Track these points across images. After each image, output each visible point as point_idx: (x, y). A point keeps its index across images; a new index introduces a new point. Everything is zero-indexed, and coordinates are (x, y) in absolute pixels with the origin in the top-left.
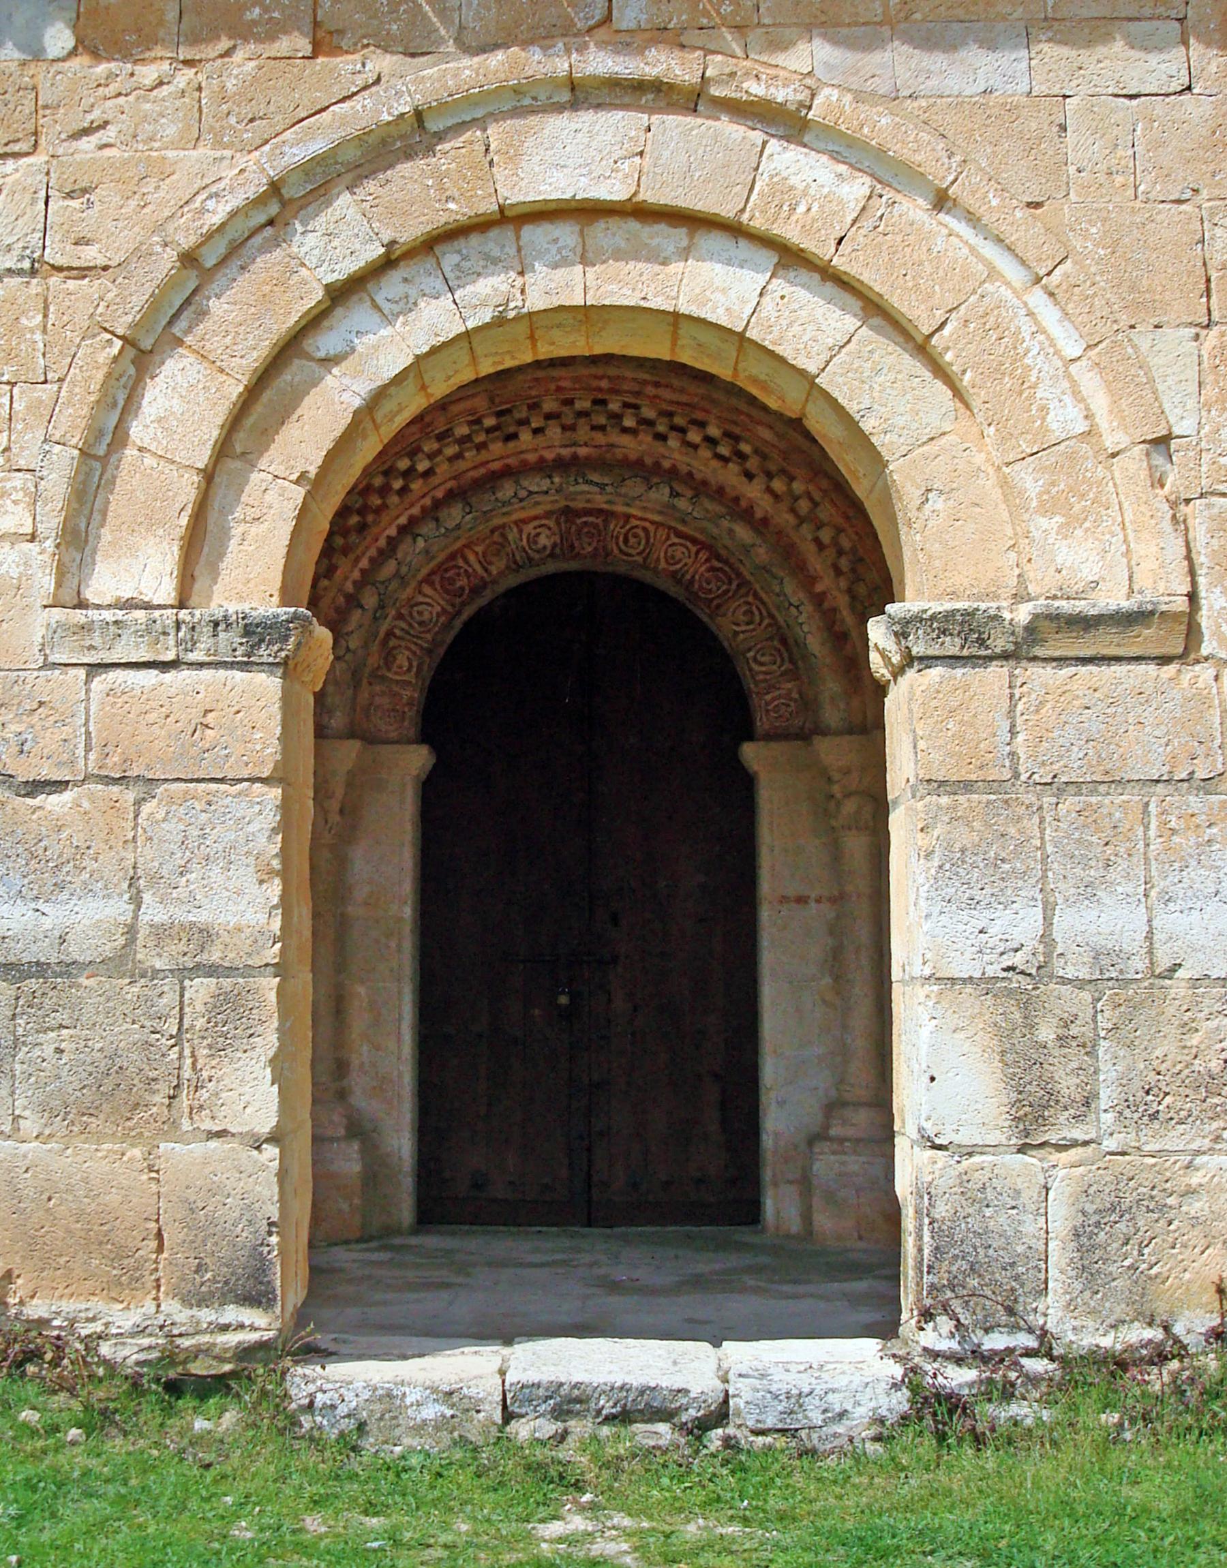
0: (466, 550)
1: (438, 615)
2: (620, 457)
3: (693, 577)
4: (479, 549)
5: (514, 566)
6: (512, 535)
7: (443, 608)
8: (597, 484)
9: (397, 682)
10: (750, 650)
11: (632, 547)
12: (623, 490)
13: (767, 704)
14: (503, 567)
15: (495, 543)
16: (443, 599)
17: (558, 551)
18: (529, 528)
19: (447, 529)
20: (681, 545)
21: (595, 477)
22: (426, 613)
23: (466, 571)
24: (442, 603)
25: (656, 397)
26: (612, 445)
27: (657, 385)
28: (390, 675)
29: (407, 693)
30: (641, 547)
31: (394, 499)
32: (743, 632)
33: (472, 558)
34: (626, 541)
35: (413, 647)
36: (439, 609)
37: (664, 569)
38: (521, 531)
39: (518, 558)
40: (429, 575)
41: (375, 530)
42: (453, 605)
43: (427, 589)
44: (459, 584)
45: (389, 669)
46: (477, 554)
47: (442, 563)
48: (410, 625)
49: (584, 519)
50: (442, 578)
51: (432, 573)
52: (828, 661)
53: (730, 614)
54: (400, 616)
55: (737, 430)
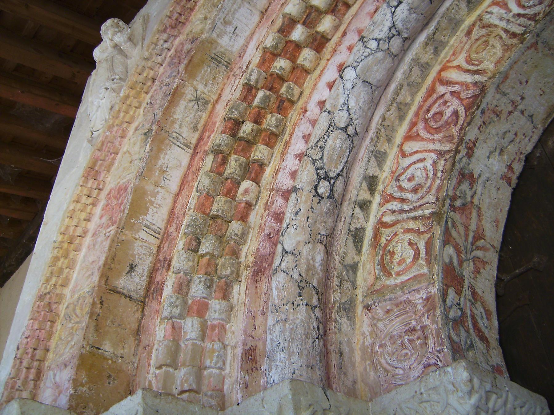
0: (443, 74)
4: (461, 60)
5: (515, 41)
9: (402, 286)
14: (499, 53)
16: (433, 141)
19: (378, 41)
22: (418, 173)
23: (452, 93)
24: (431, 146)
28: (391, 282)
29: (418, 298)
33: (453, 75)
35: (412, 225)
36: (433, 156)
40: (410, 129)
41: (300, 104)
42: (450, 139)
43: (410, 147)
44: (448, 112)
45: (390, 274)
46: (458, 67)
47: (420, 107)
48: (403, 200)
50: (426, 121)
51: (413, 124)
54: (388, 198)
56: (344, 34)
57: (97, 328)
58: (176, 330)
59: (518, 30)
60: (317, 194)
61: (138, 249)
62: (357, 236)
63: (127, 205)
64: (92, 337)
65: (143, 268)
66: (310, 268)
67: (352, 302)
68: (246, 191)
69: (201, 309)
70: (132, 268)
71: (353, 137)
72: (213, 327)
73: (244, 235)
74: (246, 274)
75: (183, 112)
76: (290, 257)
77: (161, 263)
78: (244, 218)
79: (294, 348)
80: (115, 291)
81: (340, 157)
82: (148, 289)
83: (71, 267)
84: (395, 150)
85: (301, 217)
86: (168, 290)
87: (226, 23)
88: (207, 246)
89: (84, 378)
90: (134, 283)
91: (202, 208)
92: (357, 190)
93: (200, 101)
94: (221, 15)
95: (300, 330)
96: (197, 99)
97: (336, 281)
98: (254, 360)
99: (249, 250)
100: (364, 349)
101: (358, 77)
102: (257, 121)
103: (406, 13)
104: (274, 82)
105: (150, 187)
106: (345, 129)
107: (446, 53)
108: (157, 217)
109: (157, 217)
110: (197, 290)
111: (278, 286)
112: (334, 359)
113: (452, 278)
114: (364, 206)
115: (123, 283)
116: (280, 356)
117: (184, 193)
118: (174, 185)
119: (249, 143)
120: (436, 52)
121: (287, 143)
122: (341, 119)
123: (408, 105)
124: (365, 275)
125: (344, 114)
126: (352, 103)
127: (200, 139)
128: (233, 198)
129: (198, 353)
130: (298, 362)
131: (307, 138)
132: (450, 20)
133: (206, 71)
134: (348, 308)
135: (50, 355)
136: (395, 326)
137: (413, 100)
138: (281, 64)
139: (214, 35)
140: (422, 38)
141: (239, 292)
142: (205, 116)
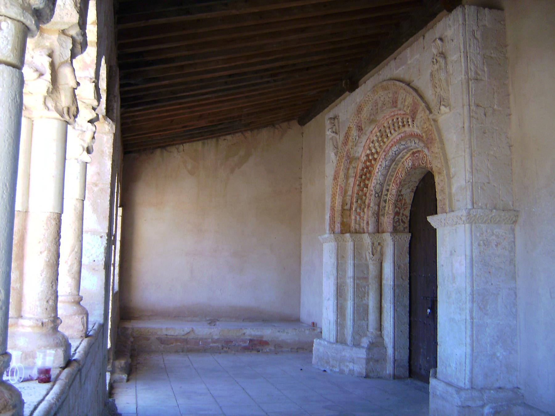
21: (403, 143)
31: (373, 162)
58: (356, 217)
61: (347, 200)
62: (385, 201)
67: (384, 213)
69: (359, 214)
73: (366, 199)
75: (351, 172)
77: (352, 203)
78: (365, 195)
80: (344, 210)
86: (354, 209)
90: (348, 207)
91: (358, 194)
92: (384, 192)
93: (354, 168)
99: (367, 201)
104: (367, 167)
107: (399, 166)
108: (350, 193)
109: (350, 193)
110: (358, 210)
111: (370, 213)
113: (397, 214)
114: (386, 195)
115: (346, 207)
118: (352, 185)
119: (364, 180)
120: (397, 165)
122: (379, 182)
129: (359, 221)
134: (383, 215)
136: (388, 220)
138: (368, 164)
141: (366, 210)
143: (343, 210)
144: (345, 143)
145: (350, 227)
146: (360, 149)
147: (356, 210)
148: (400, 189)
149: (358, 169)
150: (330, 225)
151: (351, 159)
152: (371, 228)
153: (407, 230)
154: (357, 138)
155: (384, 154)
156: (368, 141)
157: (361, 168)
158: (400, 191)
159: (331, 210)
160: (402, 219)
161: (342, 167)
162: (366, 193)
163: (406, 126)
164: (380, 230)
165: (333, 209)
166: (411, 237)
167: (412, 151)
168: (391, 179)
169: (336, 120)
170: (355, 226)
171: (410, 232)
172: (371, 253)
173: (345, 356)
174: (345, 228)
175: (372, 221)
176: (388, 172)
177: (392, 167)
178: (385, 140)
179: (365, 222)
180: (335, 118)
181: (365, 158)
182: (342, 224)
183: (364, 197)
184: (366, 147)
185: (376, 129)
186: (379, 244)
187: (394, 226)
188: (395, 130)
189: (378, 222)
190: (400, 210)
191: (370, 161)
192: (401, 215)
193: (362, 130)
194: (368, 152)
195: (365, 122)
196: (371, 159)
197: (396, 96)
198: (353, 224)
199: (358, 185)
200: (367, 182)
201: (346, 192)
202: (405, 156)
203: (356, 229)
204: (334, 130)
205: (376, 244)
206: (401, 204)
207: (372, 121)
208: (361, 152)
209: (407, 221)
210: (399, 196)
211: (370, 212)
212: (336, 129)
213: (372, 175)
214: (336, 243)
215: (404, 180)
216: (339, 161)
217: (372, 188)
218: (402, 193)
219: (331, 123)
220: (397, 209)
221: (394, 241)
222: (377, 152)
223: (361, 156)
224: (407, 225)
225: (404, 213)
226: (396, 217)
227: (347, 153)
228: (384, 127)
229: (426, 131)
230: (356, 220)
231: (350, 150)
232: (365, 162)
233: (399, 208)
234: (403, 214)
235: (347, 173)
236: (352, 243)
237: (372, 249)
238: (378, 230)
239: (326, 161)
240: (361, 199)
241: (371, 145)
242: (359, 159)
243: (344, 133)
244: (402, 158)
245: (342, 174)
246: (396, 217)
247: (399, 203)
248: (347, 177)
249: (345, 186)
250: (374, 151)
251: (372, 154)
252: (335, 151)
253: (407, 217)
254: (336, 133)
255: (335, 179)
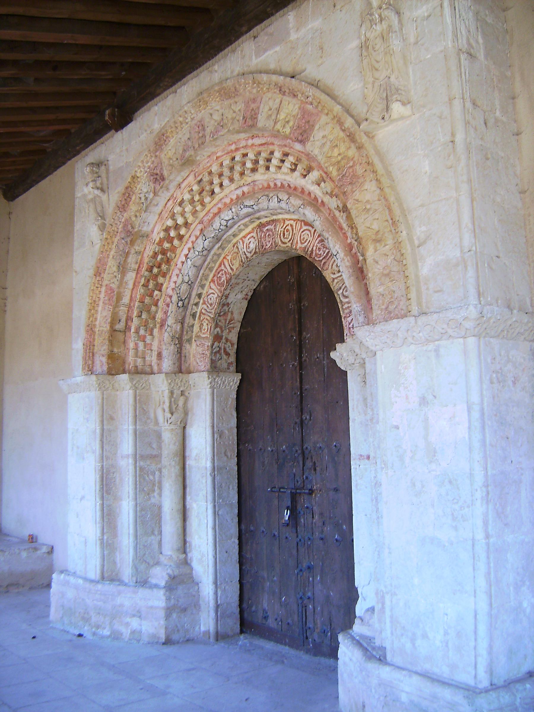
1: (216, 298)
2: (261, 187)
3: (312, 249)
4: (229, 258)
6: (240, 246)
7: (218, 295)
8: (249, 207)
10: (340, 288)
11: (286, 238)
12: (261, 206)
13: (349, 324)
15: (235, 252)
17: (257, 250)
18: (246, 241)
20: (307, 230)
21: (247, 203)
22: (212, 299)
25: (253, 145)
26: (254, 181)
27: (253, 137)
30: (290, 237)
31: (176, 242)
32: (336, 278)
34: (284, 234)
37: (300, 248)
38: (243, 243)
39: (243, 258)
41: (175, 260)
47: (217, 269)
49: (267, 228)
52: (352, 289)
53: (330, 267)
54: (204, 303)
55: (287, 150)
56: (190, 237)
57: (112, 345)
58: (136, 344)
59: (244, 261)
60: (178, 306)
61: (121, 313)
62: (194, 316)
63: (114, 299)
64: (110, 348)
65: (123, 320)
66: (176, 332)
67: (191, 338)
68: (157, 295)
70: (120, 321)
71: (191, 285)
72: (148, 344)
73: (156, 312)
74: (158, 326)
75: (132, 260)
76: (169, 328)
77: (129, 319)
78: (156, 305)
79: (170, 358)
81: (186, 292)
82: (126, 327)
83: (97, 313)
84: (208, 283)
85: (173, 314)
86: (133, 330)
87: (144, 222)
88: (144, 316)
89: (110, 362)
90: (120, 326)
91: (142, 302)
92: (194, 299)
93: (137, 253)
94: (142, 221)
95: (172, 353)
96: (136, 252)
97: (185, 333)
98: (161, 356)
99: (159, 316)
100: (193, 354)
101: (192, 264)
102: (159, 267)
103: (208, 244)
104: (164, 252)
105: (122, 290)
106: (188, 283)
108: (126, 300)
109: (126, 300)
110: (142, 332)
112: (183, 358)
113: (217, 338)
114: (197, 304)
116: (166, 360)
117: (135, 289)
118: (131, 286)
119: (156, 276)
120: (223, 249)
121: (170, 277)
122: (186, 279)
123: (213, 267)
124: (196, 329)
125: (187, 277)
126: (190, 273)
127: (139, 267)
128: (152, 297)
129: (144, 352)
130: (171, 362)
131: (175, 282)
132: (227, 241)
133: (139, 241)
134: (189, 341)
135: (96, 348)
136: (200, 350)
137: (215, 265)
138: (166, 245)
139: (140, 228)
140: (217, 246)
141: (156, 331)
142: (140, 257)
143: (113, 331)
144: (123, 207)
145: (124, 362)
146: (152, 218)
147: (137, 332)
148: (227, 292)
149: (145, 255)
150: (84, 359)
151: (132, 235)
152: (167, 364)
153: (233, 368)
154: (151, 195)
155: (200, 227)
156: (171, 202)
157: (151, 253)
158: (227, 297)
159: (87, 331)
160: (225, 349)
161: (112, 253)
162: (158, 300)
163: (261, 170)
164: (184, 368)
165: (91, 329)
166: (241, 380)
167: (257, 222)
168: (208, 275)
169: (103, 168)
170: (135, 361)
171: (237, 372)
172: (167, 410)
173: (122, 605)
174: (116, 366)
175: (168, 352)
176: (204, 261)
177: (212, 252)
178: (207, 200)
179: (155, 354)
180: (99, 164)
181: (162, 235)
182: (111, 356)
183: (153, 308)
184: (165, 215)
185: (191, 178)
186: (182, 393)
187: (211, 359)
188: (231, 180)
189: (180, 355)
190: (222, 332)
191: (170, 240)
192: (224, 340)
193: (163, 179)
194: (170, 223)
195: (172, 166)
196: (173, 236)
197: (253, 106)
198: (130, 359)
199: (143, 285)
200: (161, 280)
201: (119, 297)
202: (241, 231)
203: (136, 367)
204: (98, 184)
205: (177, 392)
206: (226, 320)
207: (187, 162)
208: (154, 225)
209: (233, 351)
210: (224, 305)
211: (166, 335)
212: (102, 184)
213: (172, 268)
214: (99, 393)
215: (237, 277)
216: (107, 242)
217: (170, 292)
218: (229, 300)
219: (92, 172)
220: (218, 329)
221: (212, 388)
222: (186, 224)
223: (153, 232)
224: (233, 359)
225: (229, 338)
226: (216, 344)
227: (125, 226)
228: (210, 173)
229: (339, 162)
230: (136, 349)
231: (134, 219)
232: (161, 242)
233: (221, 328)
234: (227, 340)
235: (125, 261)
236: (131, 392)
237: (170, 402)
238: (181, 368)
239: (76, 244)
240: (149, 311)
241: (178, 209)
242: (147, 236)
243: (121, 189)
244: (234, 236)
245: (112, 265)
246: (216, 344)
247: (221, 318)
248: (122, 269)
249: (119, 287)
250: (180, 221)
251: (177, 227)
252: (99, 222)
253: (232, 345)
254: (102, 190)
255: (98, 273)
